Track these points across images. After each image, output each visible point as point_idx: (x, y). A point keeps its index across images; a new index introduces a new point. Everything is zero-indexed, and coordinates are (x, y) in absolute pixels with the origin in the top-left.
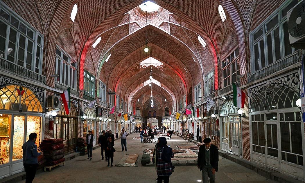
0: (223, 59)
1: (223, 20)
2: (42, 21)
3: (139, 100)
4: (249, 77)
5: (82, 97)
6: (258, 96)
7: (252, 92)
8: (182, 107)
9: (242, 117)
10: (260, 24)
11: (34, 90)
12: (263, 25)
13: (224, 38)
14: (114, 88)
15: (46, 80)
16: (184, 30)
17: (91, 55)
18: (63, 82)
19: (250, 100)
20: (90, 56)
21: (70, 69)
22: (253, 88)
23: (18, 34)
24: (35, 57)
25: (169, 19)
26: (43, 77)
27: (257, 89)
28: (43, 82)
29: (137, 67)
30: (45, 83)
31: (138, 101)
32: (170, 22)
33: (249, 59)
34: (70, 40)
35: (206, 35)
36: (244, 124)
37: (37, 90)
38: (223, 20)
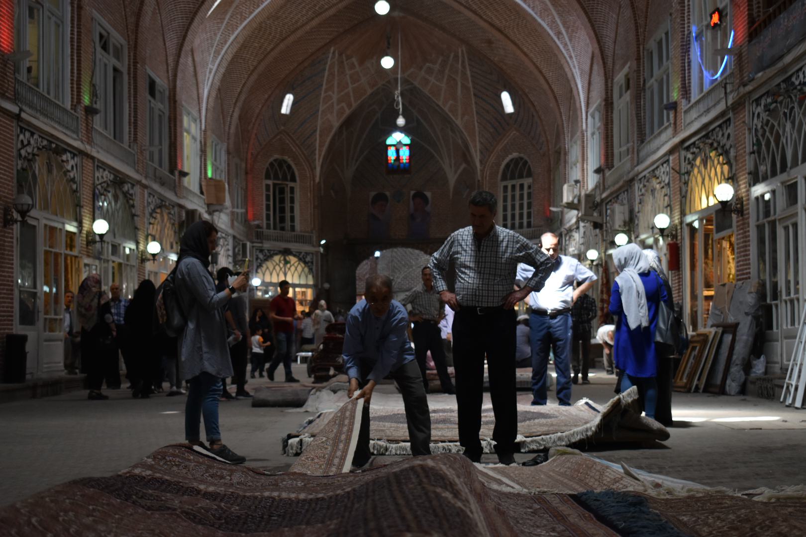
3: (289, 99)
8: (675, 95)
31: (285, 109)
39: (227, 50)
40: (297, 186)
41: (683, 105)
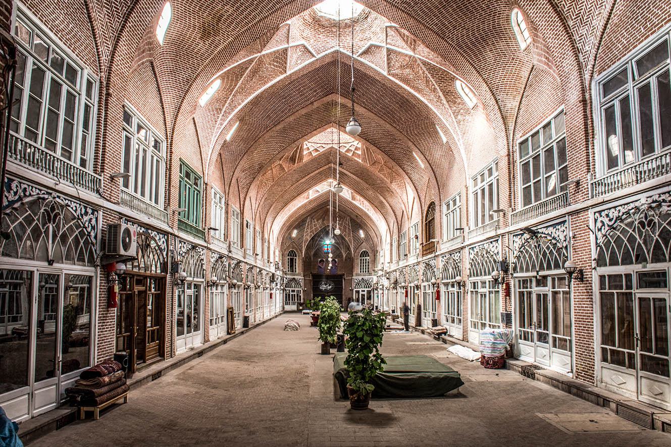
0: (521, 137)
1: (523, 46)
2: (96, 44)
4: (592, 184)
5: (176, 224)
6: (618, 230)
7: (600, 219)
9: (575, 279)
10: (620, 59)
11: (79, 210)
12: (627, 63)
13: (525, 88)
14: (242, 203)
15: (102, 185)
16: (421, 65)
17: (195, 123)
18: (136, 191)
19: (596, 239)
20: (192, 126)
21: (150, 158)
22: (604, 210)
23: (49, 76)
24: (81, 128)
26: (97, 178)
27: (614, 214)
28: (98, 191)
29: (296, 151)
30: (100, 194)
32: (389, 46)
33: (593, 140)
34: (152, 87)
35: (480, 79)
36: (578, 296)
37: (83, 210)
38: (523, 46)
39: (281, 224)
40: (297, 258)
41: (409, 255)
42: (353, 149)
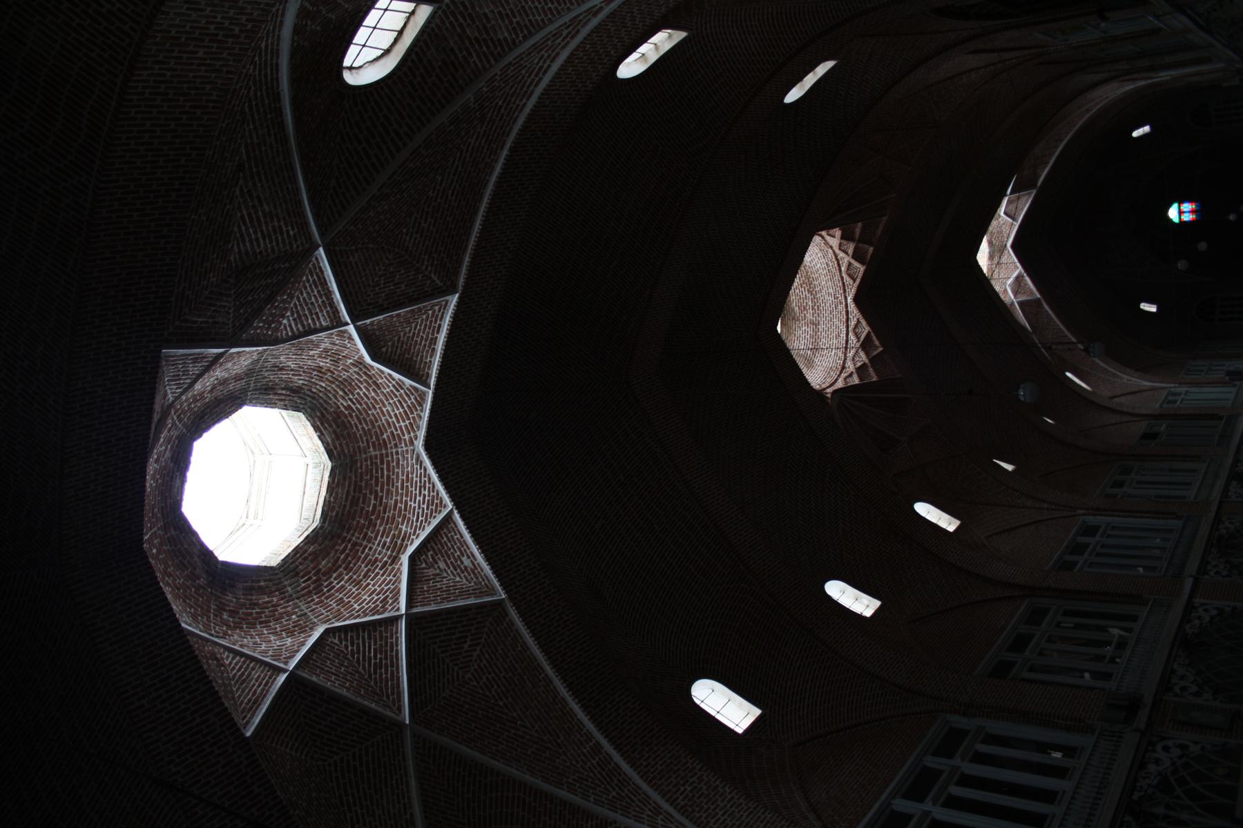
25: (316, 331)
42: (851, 248)
